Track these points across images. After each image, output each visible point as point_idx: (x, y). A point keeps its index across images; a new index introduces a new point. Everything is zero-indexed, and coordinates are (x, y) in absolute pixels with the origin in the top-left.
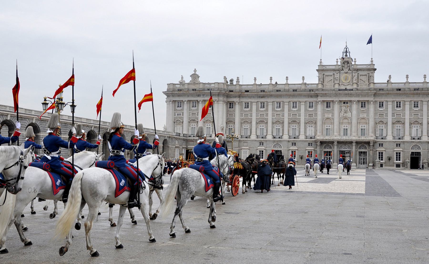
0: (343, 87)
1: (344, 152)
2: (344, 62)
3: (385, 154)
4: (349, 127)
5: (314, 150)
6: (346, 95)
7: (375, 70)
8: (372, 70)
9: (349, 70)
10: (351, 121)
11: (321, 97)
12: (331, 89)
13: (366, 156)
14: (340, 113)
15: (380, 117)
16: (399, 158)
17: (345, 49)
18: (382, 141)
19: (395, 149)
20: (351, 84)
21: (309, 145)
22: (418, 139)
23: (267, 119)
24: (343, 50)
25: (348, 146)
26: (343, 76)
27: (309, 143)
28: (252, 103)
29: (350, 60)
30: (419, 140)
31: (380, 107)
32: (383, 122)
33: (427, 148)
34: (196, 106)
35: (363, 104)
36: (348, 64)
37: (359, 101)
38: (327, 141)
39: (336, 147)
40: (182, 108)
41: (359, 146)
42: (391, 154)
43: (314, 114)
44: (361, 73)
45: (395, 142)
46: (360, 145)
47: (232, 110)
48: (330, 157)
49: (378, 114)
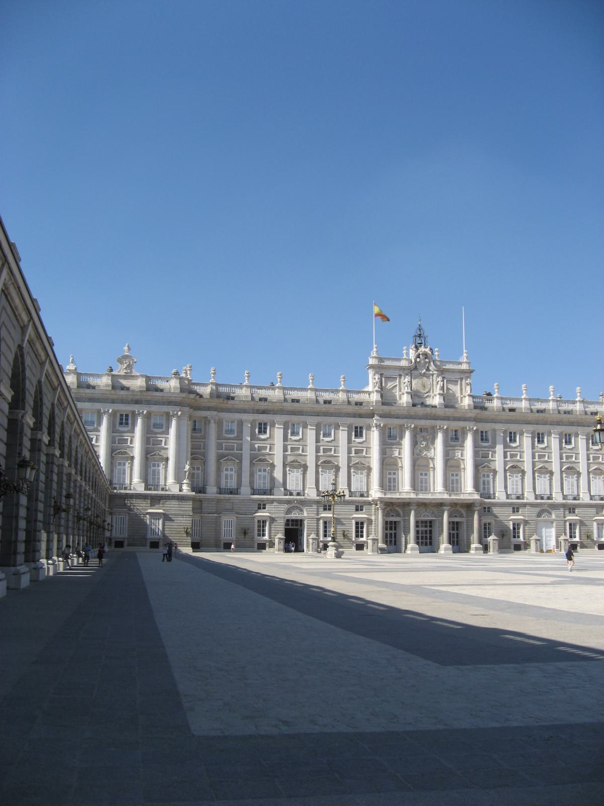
0: (417, 401)
2: (419, 354)
7: (472, 372)
8: (468, 372)
9: (427, 370)
10: (434, 465)
15: (483, 459)
17: (418, 333)
18: (490, 503)
20: (432, 395)
22: (549, 498)
24: (414, 331)
25: (431, 512)
27: (357, 507)
28: (241, 423)
29: (427, 350)
30: (550, 501)
31: (482, 439)
33: (563, 515)
34: (127, 424)
38: (399, 501)
39: (413, 513)
44: (447, 375)
48: (391, 532)
49: (481, 452)
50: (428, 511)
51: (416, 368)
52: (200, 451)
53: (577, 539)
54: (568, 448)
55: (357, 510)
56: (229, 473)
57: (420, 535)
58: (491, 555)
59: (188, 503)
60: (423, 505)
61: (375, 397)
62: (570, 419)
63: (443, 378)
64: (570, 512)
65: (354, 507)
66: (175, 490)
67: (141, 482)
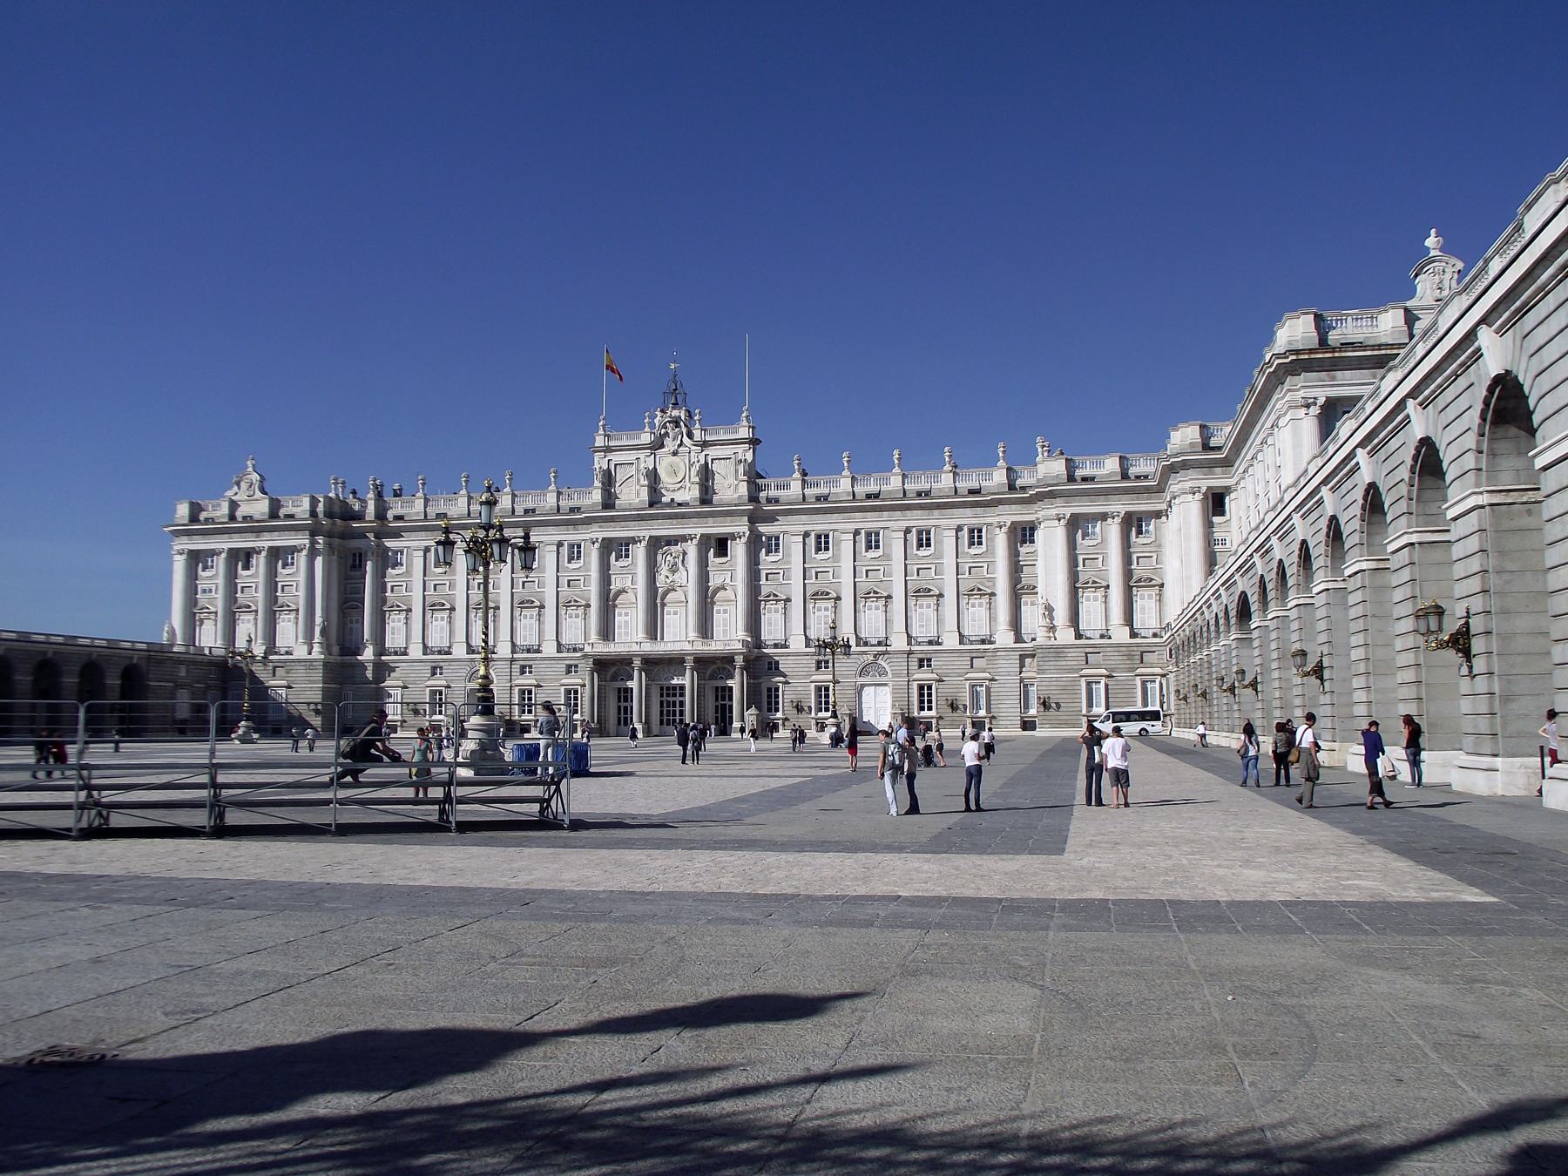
2: (666, 423)
8: (742, 443)
9: (680, 446)
11: (600, 527)
12: (630, 504)
15: (769, 583)
22: (879, 644)
23: (451, 599)
26: (664, 462)
35: (721, 545)
40: (214, 573)
41: (708, 673)
42: (802, 692)
44: (713, 452)
46: (715, 666)
47: (358, 573)
51: (662, 446)
52: (356, 596)
53: (933, 713)
54: (437, 572)
55: (569, 672)
56: (396, 624)
57: (678, 709)
58: (736, 740)
59: (317, 671)
61: (597, 496)
64: (921, 666)
65: (562, 666)
66: (301, 652)
67: (264, 644)
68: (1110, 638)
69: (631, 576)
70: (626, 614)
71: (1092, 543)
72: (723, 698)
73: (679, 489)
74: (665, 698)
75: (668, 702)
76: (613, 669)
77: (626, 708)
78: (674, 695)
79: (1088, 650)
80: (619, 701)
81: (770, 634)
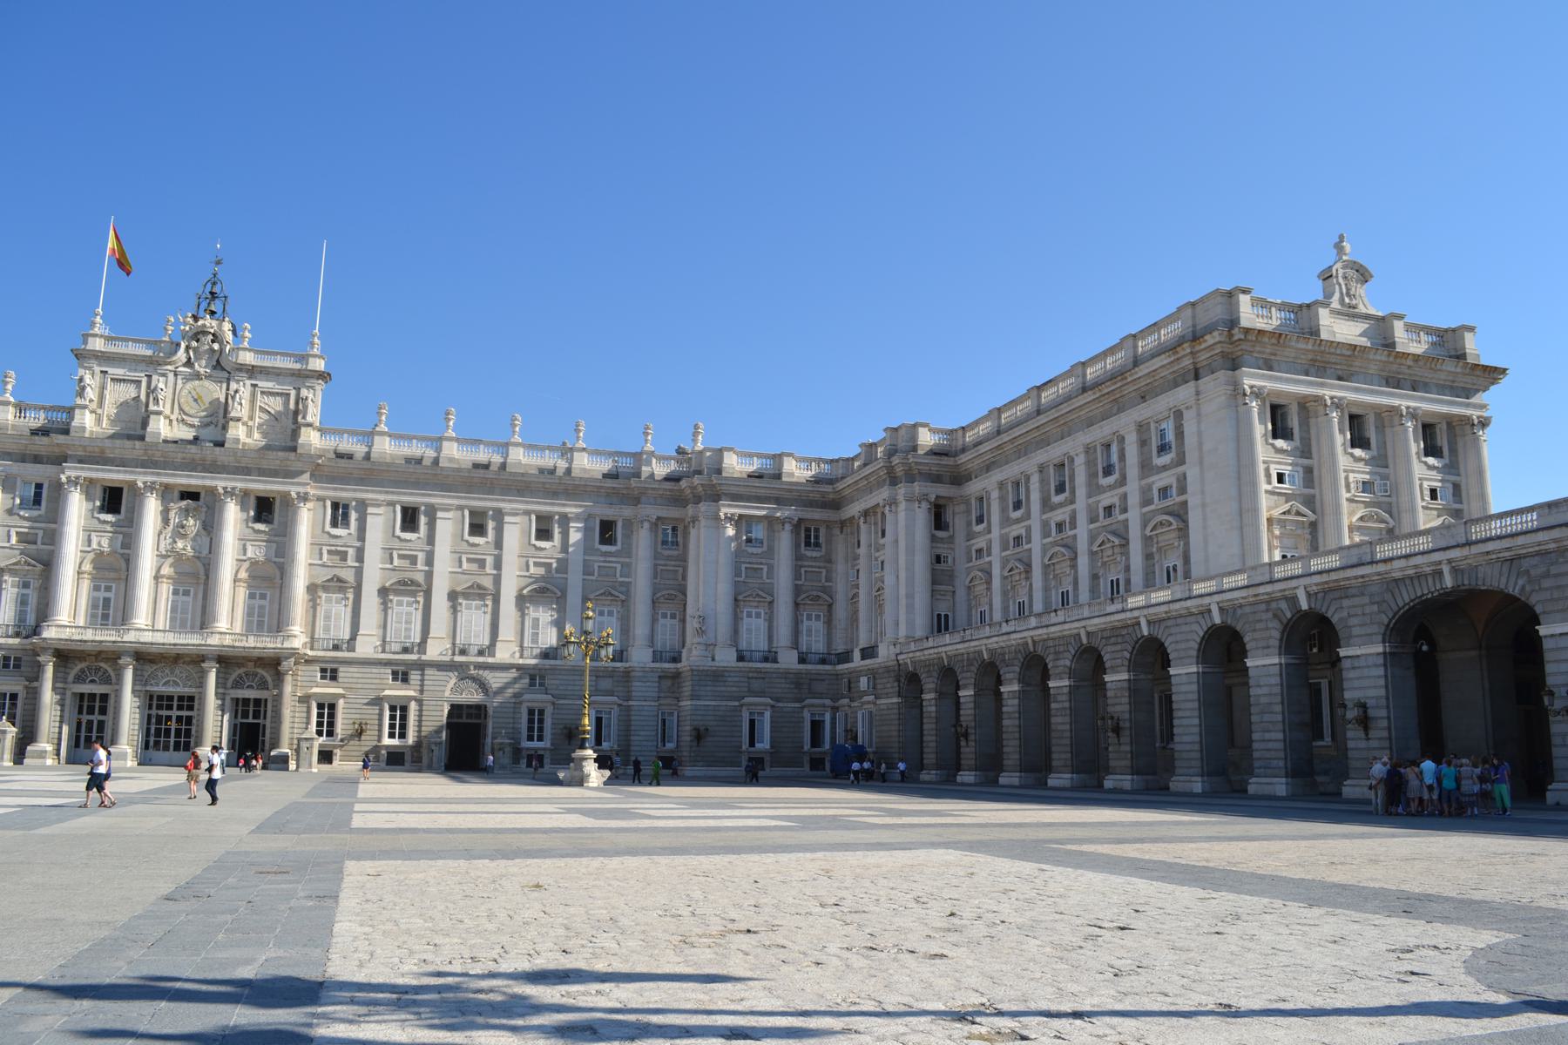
1: (170, 698)
3: (345, 711)
4: (196, 594)
5: (26, 687)
6: (192, 466)
11: (80, 462)
13: (265, 718)
14: (162, 537)
16: (403, 727)
17: (209, 285)
19: (387, 692)
20: (222, 421)
21: (6, 666)
22: (481, 653)
24: (199, 287)
30: (481, 659)
32: (340, 580)
36: (213, 341)
37: (246, 493)
38: (88, 647)
39: (129, 675)
41: (231, 681)
43: (41, 533)
45: (387, 663)
46: (241, 671)
48: (101, 718)
50: (177, 672)
53: (546, 744)
60: (145, 658)
62: (547, 486)
63: (254, 386)
68: (775, 661)
69: (121, 536)
70: (108, 589)
71: (755, 550)
72: (245, 715)
73: (207, 425)
74: (154, 712)
75: (159, 718)
76: (83, 665)
77: (90, 723)
78: (170, 707)
79: (751, 675)
80: (80, 712)
81: (327, 629)
